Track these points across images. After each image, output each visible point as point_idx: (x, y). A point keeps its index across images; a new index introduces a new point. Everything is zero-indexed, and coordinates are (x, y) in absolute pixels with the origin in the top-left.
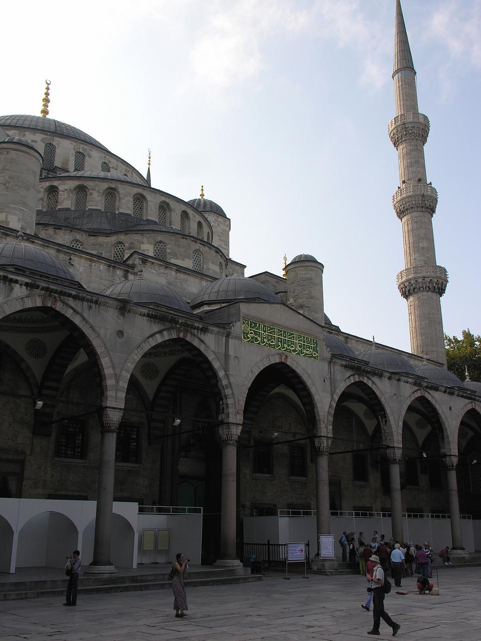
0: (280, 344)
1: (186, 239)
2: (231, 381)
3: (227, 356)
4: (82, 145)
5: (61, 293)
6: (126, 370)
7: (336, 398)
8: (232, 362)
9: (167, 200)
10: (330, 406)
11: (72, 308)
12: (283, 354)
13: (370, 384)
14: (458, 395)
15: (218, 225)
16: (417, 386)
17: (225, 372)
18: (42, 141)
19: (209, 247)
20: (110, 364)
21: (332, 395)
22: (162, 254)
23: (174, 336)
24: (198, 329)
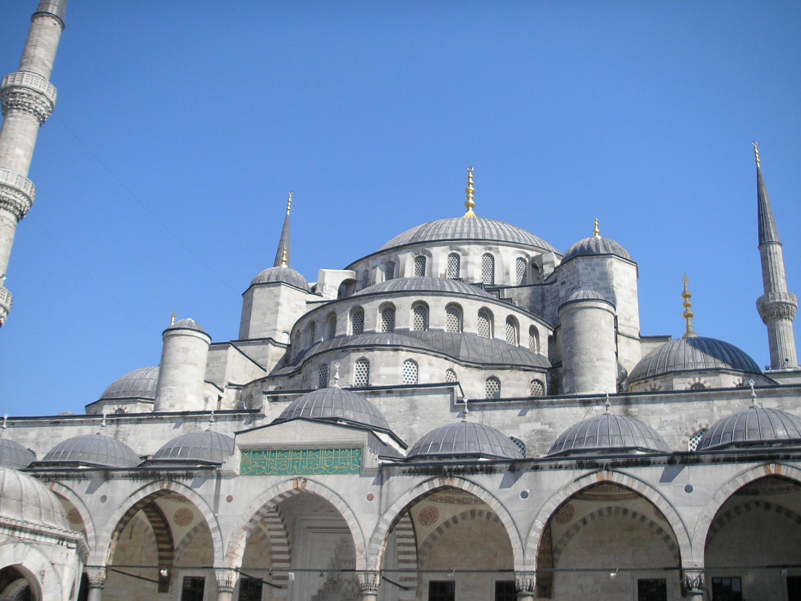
0: (296, 467)
1: (346, 351)
2: (220, 523)
3: (217, 497)
4: (420, 249)
5: (57, 477)
6: (107, 531)
7: (390, 517)
8: (223, 501)
9: (389, 300)
10: (377, 530)
11: (65, 486)
12: (300, 478)
13: (466, 486)
14: (715, 461)
15: (593, 270)
16: (587, 468)
17: (214, 514)
18: (382, 263)
19: (379, 350)
20: (92, 528)
21: (381, 515)
22: (361, 373)
23: (157, 488)
24: (183, 476)
